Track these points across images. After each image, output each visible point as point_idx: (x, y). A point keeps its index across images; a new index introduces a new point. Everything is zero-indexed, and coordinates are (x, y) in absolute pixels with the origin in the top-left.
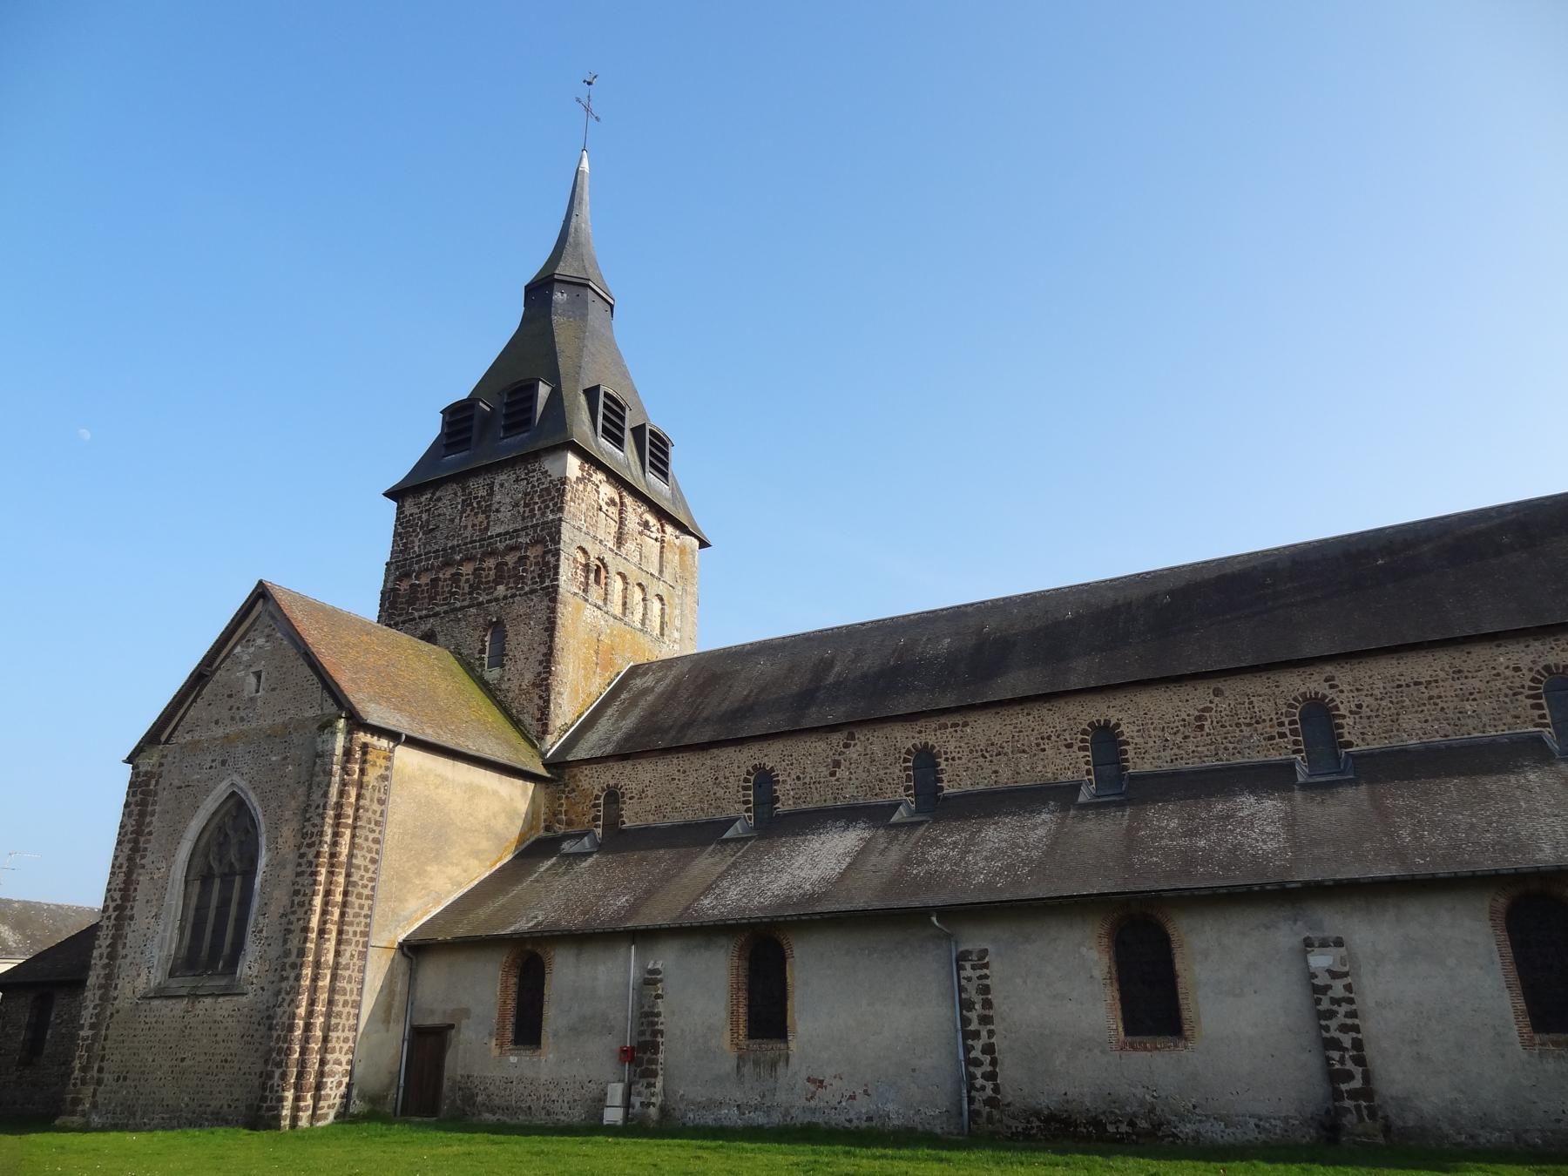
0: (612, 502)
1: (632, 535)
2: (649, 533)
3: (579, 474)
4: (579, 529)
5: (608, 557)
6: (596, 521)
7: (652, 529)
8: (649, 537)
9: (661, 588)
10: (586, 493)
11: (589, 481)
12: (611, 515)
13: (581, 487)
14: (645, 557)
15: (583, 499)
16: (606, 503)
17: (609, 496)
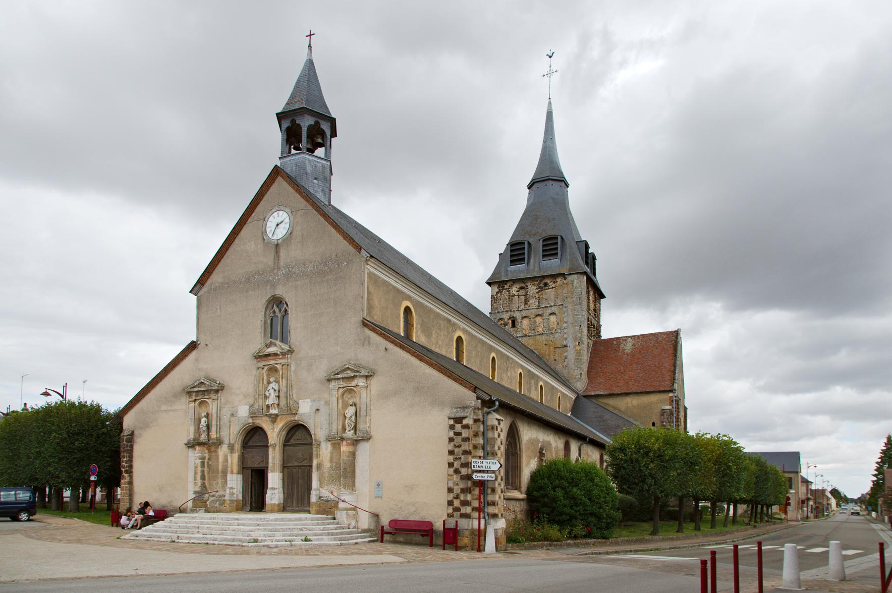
0: (522, 288)
1: (532, 296)
2: (547, 288)
3: (498, 290)
4: (498, 312)
5: (517, 315)
6: (509, 304)
7: (550, 284)
8: (549, 289)
9: (554, 309)
10: (502, 296)
11: (503, 289)
12: (522, 294)
13: (499, 295)
14: (546, 299)
15: (500, 299)
16: (517, 291)
17: (518, 287)
